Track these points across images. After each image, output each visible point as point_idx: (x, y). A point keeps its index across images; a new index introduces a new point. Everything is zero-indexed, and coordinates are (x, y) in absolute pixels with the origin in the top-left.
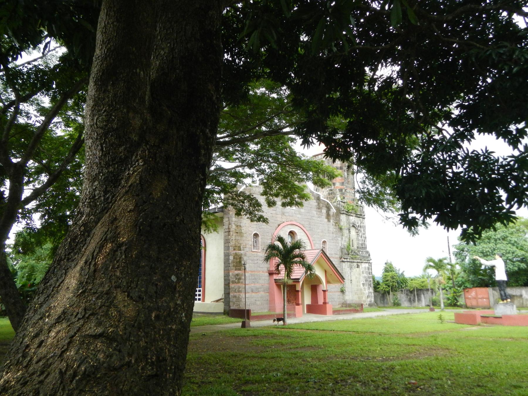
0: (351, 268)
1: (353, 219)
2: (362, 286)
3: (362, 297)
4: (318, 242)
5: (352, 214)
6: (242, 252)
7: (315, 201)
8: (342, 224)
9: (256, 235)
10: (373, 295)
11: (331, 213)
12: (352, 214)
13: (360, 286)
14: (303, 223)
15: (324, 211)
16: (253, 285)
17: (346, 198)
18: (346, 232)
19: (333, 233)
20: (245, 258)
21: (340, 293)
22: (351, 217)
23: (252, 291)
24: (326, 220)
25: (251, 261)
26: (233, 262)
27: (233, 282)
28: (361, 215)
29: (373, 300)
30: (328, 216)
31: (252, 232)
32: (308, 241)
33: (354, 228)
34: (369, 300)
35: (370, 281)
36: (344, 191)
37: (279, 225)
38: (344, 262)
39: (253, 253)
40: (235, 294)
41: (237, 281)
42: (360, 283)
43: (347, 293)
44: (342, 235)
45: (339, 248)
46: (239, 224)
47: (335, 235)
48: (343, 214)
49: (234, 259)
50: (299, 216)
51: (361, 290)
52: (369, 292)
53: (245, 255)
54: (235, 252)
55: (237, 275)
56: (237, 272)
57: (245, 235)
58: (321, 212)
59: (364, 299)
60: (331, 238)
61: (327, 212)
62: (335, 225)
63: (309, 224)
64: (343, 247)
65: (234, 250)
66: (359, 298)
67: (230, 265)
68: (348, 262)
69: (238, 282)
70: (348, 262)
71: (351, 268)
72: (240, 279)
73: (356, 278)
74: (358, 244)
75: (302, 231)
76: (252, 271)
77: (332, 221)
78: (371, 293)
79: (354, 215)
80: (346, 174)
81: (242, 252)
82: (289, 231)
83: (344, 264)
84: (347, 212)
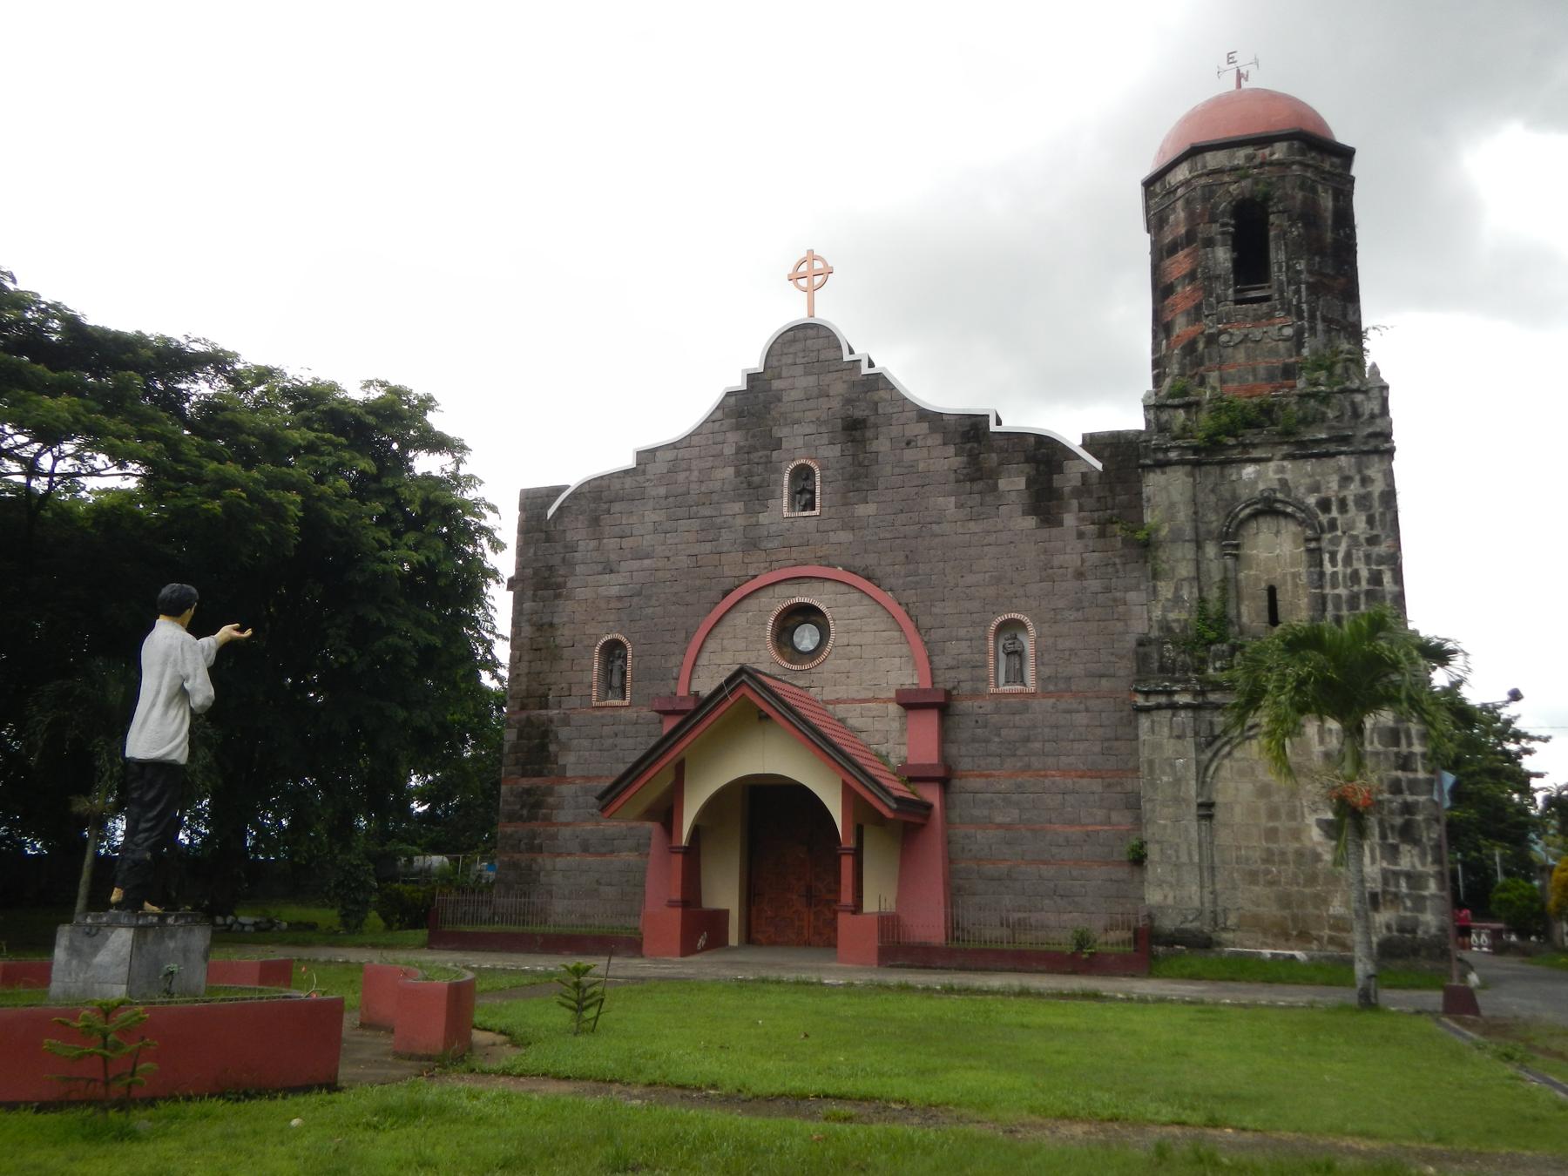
0: (1210, 742)
1: (1255, 476)
2: (1316, 834)
3: (1322, 900)
4: (962, 632)
5: (1256, 454)
6: (553, 712)
7: (951, 450)
8: (1149, 518)
9: (613, 650)
10: (1432, 887)
11: (1069, 479)
12: (1256, 454)
13: (1296, 834)
14: (870, 560)
15: (1014, 483)
16: (589, 827)
17: (1213, 378)
18: (1180, 559)
19: (1080, 575)
20: (564, 733)
21: (1122, 873)
22: (1249, 471)
23: (585, 848)
24: (1031, 522)
25: (586, 743)
26: (515, 748)
27: (513, 817)
28: (1345, 440)
29: (1430, 920)
30: (1044, 502)
31: (598, 639)
32: (897, 634)
33: (1292, 527)
34: (1383, 917)
35: (1408, 808)
36: (1201, 346)
37: (726, 594)
38: (1147, 710)
39: (598, 713)
40: (517, 856)
41: (525, 812)
42: (1292, 815)
43: (1156, 868)
44: (1156, 575)
45: (1130, 641)
46: (546, 620)
47: (1094, 584)
48: (1162, 465)
49: (520, 737)
50: (844, 536)
51: (1308, 857)
52: (1388, 877)
53: (566, 721)
54: (524, 715)
55: (528, 792)
56: (525, 783)
57: (567, 653)
58: (995, 488)
59: (1337, 908)
60: (1061, 604)
61: (1029, 483)
62: (1102, 534)
63: (908, 560)
64: (1155, 633)
65: (523, 707)
66: (1285, 901)
67: (505, 761)
68: (1174, 707)
69: (532, 818)
70: (1174, 707)
71: (1210, 742)
72: (538, 805)
73: (1264, 791)
74: (1320, 603)
75: (857, 595)
76: (587, 778)
77: (1070, 520)
78: (1415, 879)
79: (1285, 449)
80: (1223, 256)
81: (553, 712)
82: (780, 608)
83: (1144, 722)
84: (1196, 450)
